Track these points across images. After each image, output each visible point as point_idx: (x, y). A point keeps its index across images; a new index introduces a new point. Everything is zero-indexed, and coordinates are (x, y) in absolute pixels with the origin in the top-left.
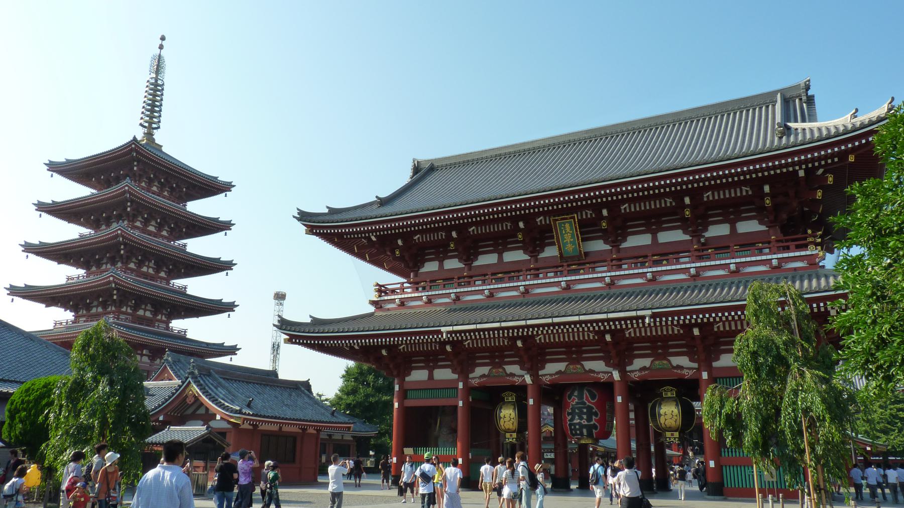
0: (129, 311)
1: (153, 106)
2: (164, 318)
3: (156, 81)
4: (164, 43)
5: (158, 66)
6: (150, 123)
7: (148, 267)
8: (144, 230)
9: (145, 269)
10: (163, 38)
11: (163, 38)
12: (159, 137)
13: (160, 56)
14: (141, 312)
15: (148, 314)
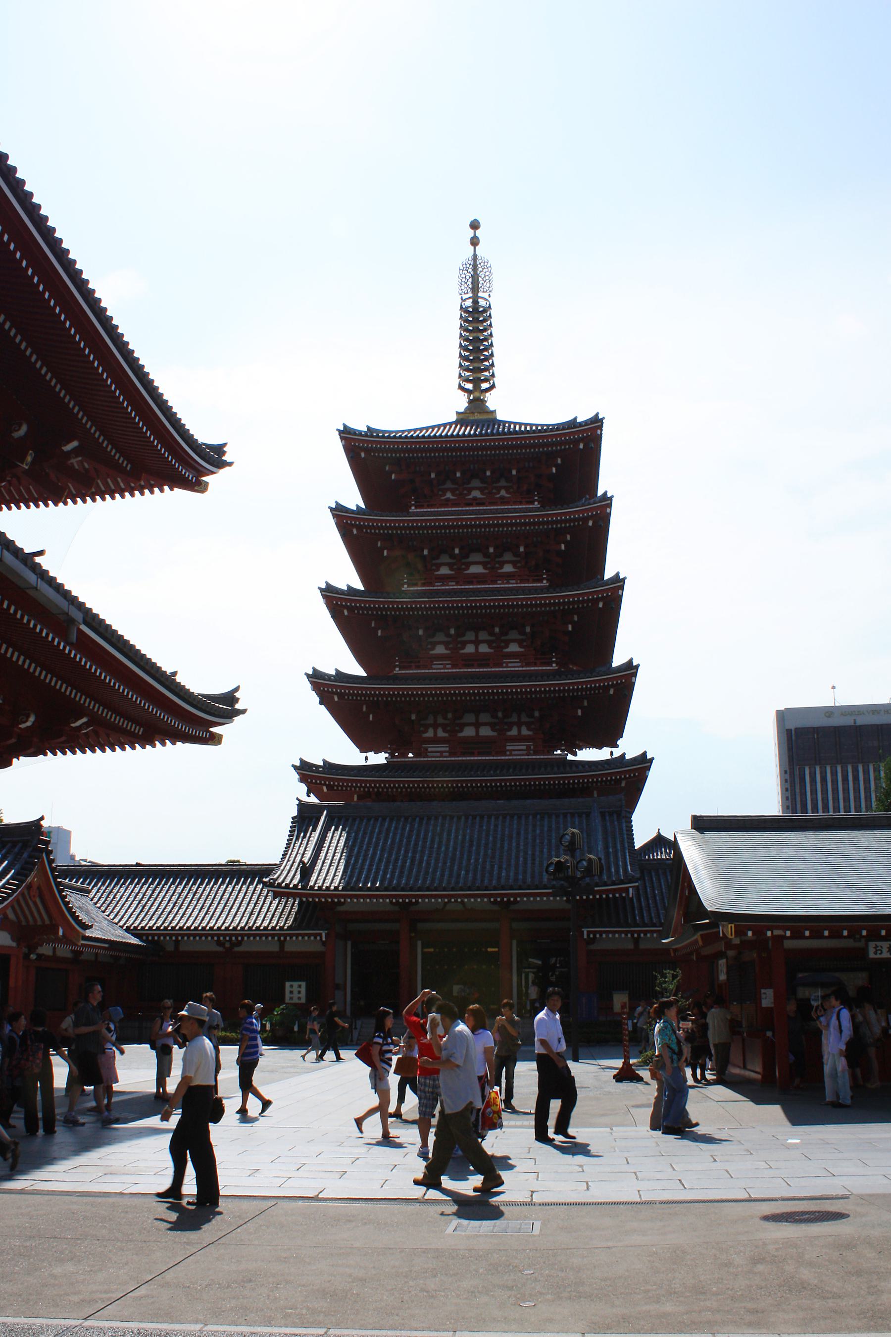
0: (441, 733)
1: (477, 351)
2: (525, 732)
3: (476, 302)
4: (478, 233)
5: (475, 278)
6: (477, 382)
7: (477, 643)
8: (459, 576)
9: (470, 649)
10: (475, 225)
11: (475, 225)
12: (492, 401)
13: (475, 257)
14: (469, 732)
15: (485, 732)
